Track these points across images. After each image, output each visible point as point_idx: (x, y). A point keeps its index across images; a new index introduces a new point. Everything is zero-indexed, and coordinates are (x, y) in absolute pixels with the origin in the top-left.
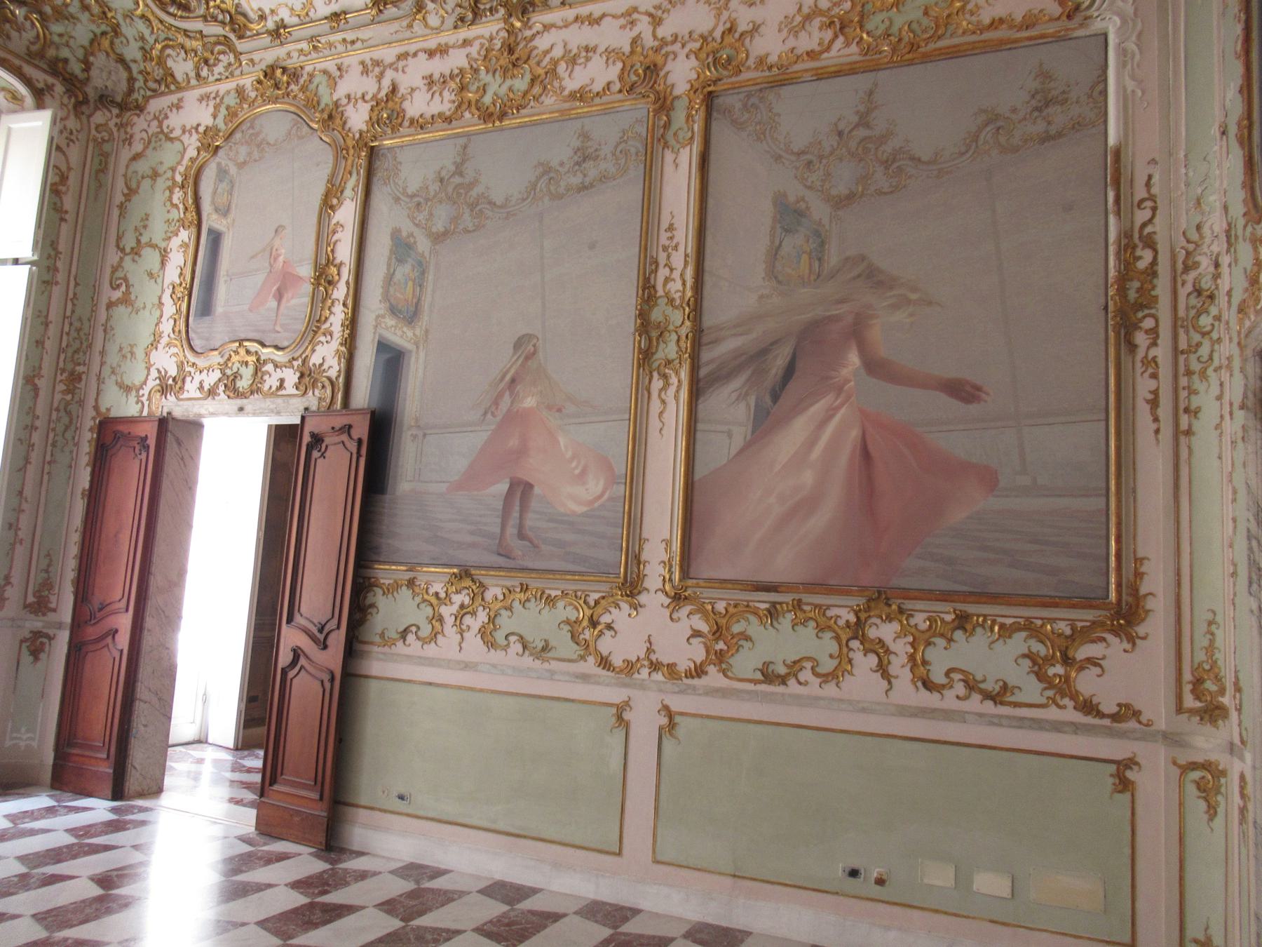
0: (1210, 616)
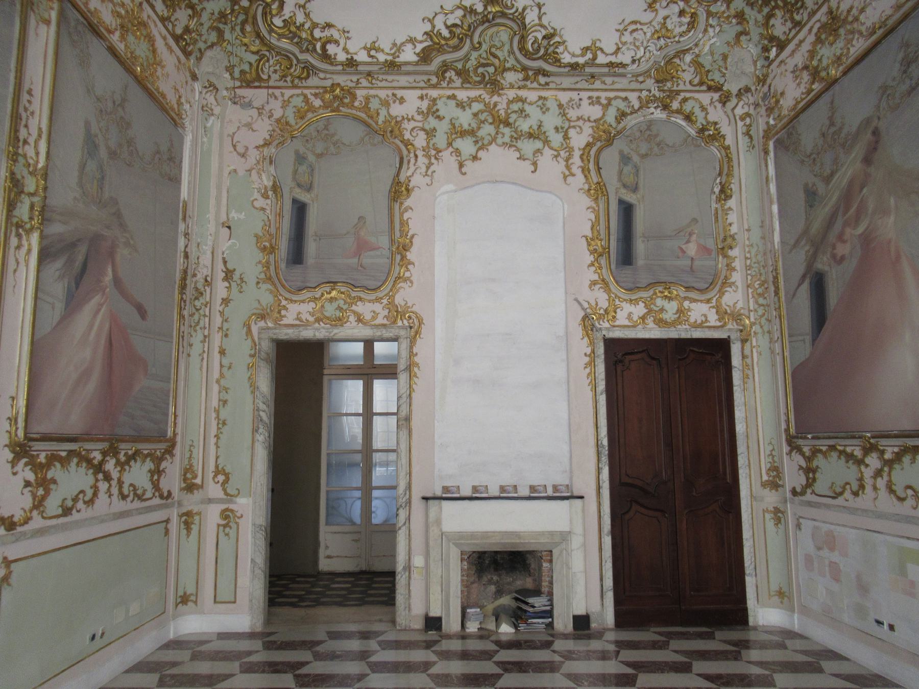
0: (190, 443)
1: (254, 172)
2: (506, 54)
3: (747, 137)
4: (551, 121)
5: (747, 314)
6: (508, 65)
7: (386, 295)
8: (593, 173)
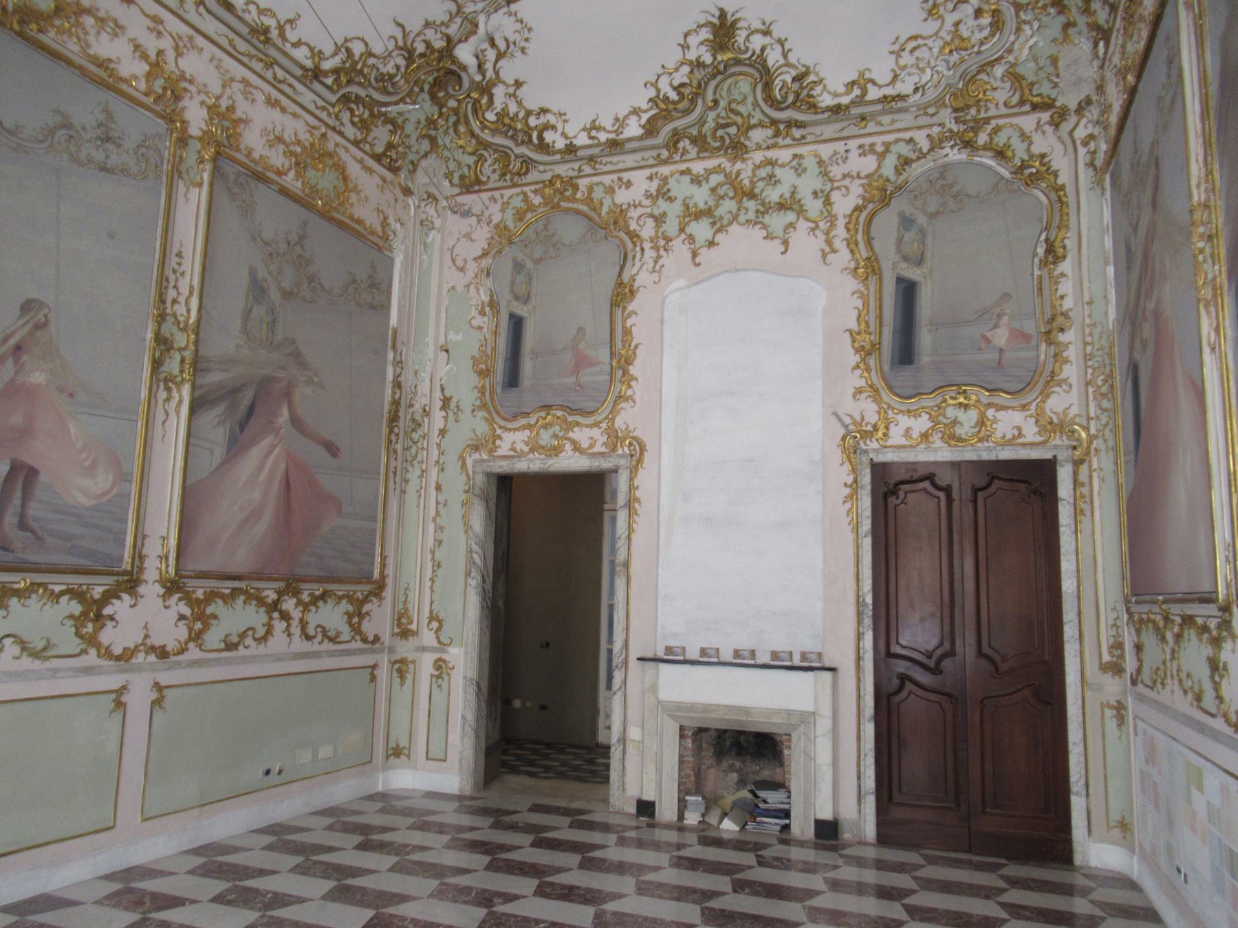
0: (406, 586)
1: (472, 288)
2: (750, 107)
3: (1091, 169)
4: (808, 184)
5: (1085, 423)
6: (753, 121)
7: (606, 418)
8: (861, 245)
